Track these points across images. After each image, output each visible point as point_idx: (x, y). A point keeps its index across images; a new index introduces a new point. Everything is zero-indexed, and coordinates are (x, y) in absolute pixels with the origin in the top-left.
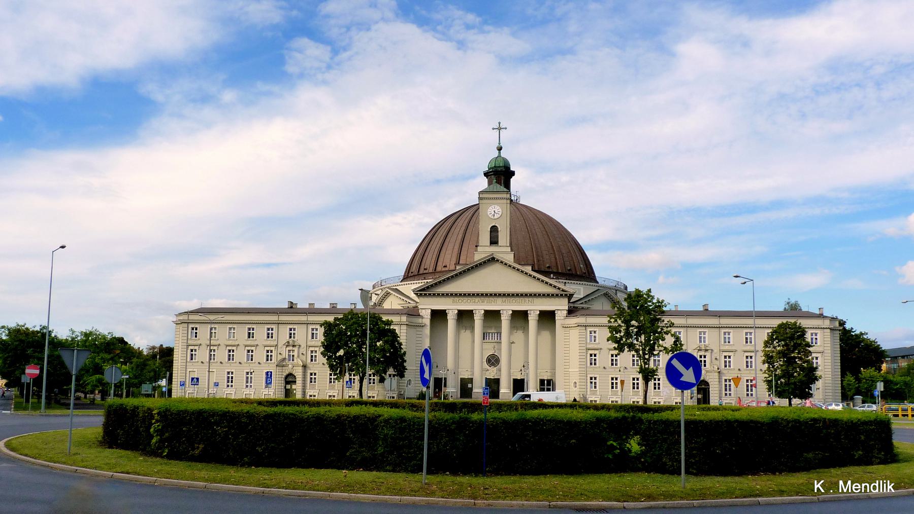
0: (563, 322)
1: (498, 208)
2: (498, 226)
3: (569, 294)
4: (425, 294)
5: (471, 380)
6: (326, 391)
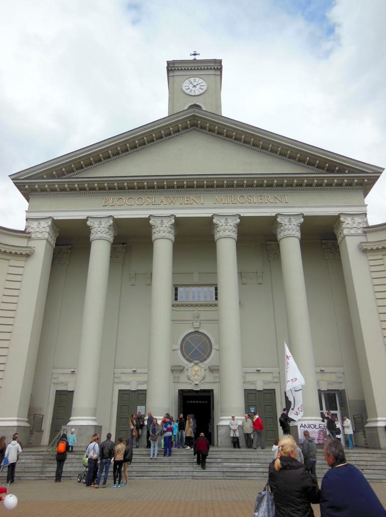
0: (363, 239)
1: (201, 81)
5: (140, 396)
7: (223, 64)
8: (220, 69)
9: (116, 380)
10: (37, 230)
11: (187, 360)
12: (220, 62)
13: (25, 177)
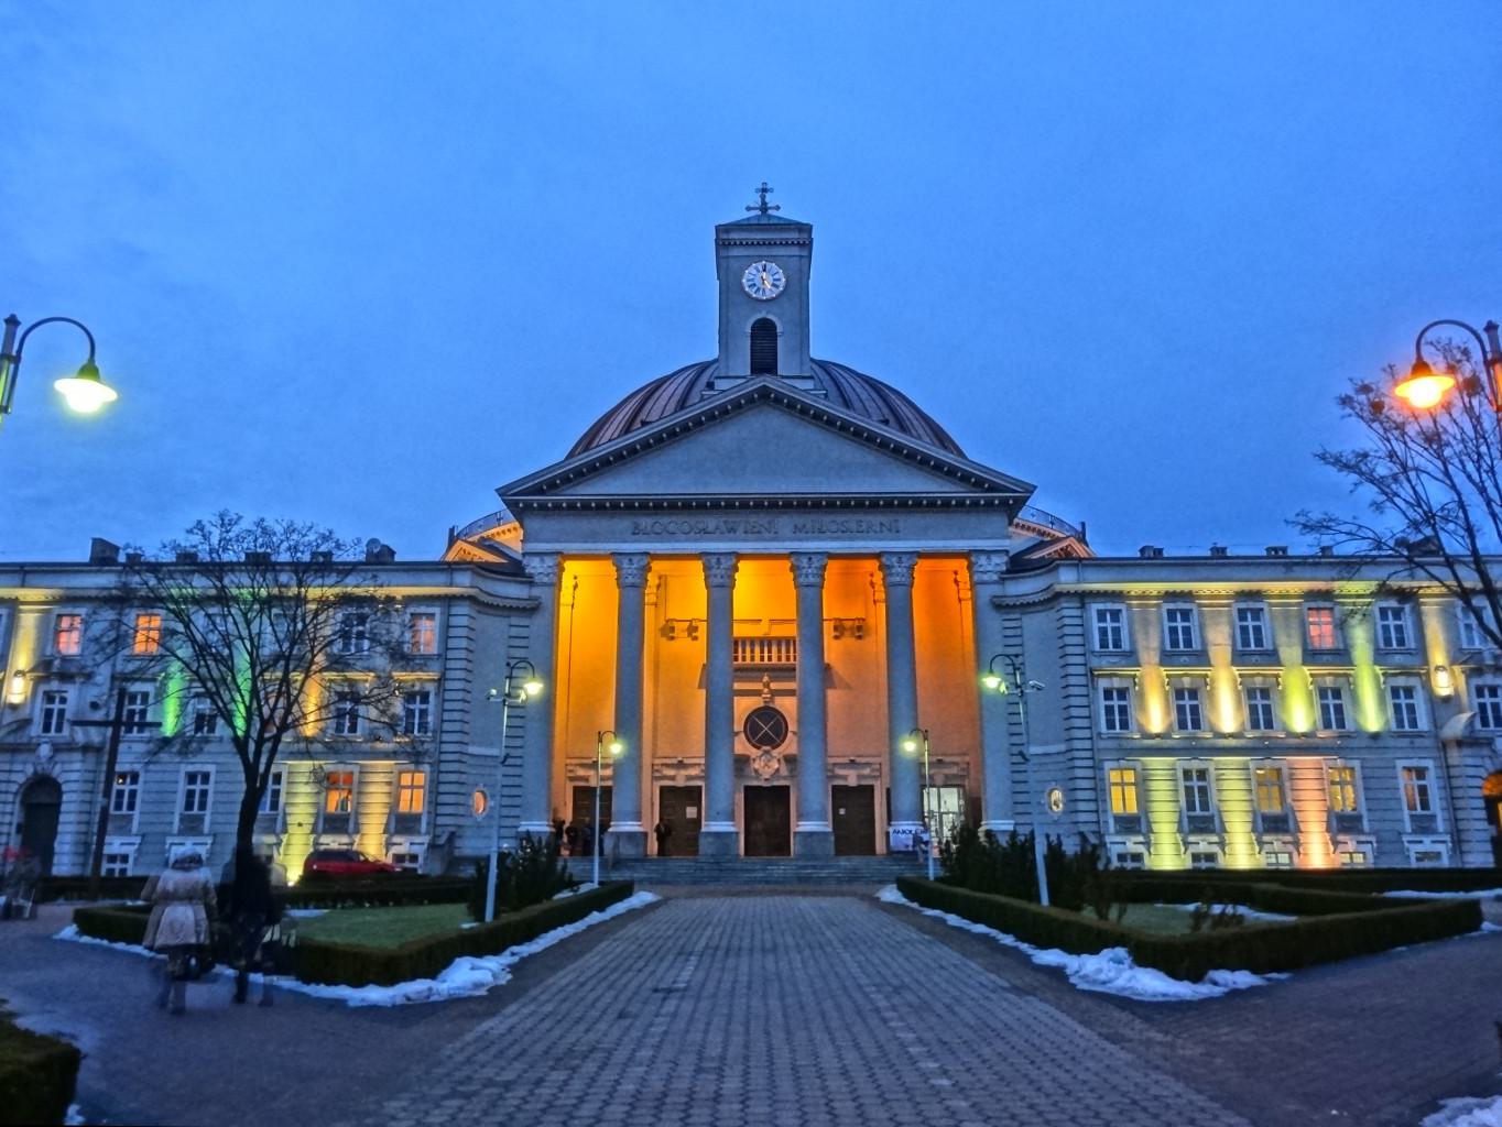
0: (996, 590)
2: (770, 317)
3: (1015, 499)
4: (543, 507)
6: (169, 840)
7: (814, 235)
8: (807, 245)
9: (657, 774)
10: (541, 570)
11: (754, 746)
12: (806, 229)
13: (516, 490)
